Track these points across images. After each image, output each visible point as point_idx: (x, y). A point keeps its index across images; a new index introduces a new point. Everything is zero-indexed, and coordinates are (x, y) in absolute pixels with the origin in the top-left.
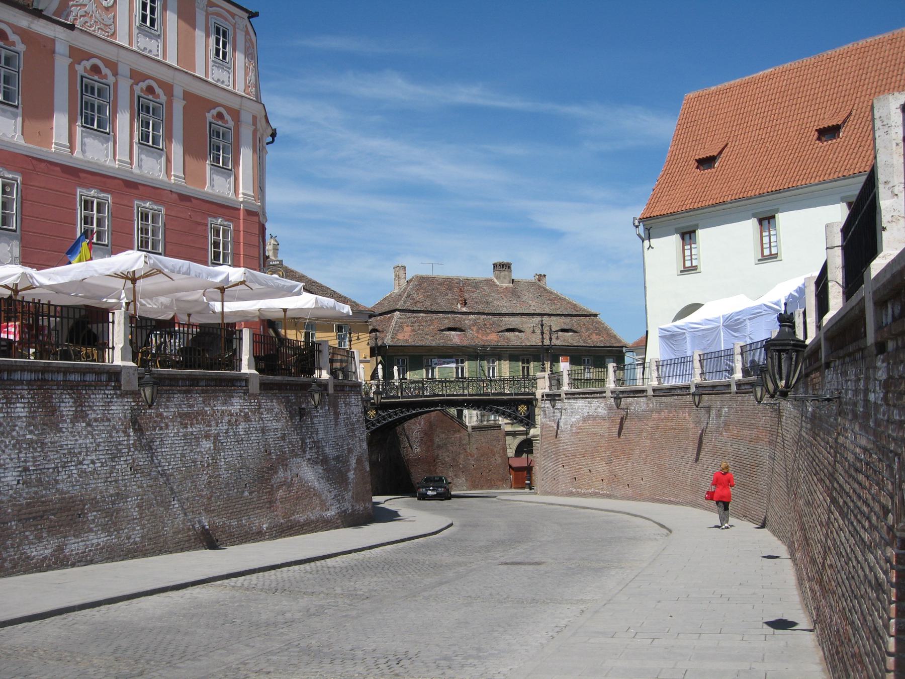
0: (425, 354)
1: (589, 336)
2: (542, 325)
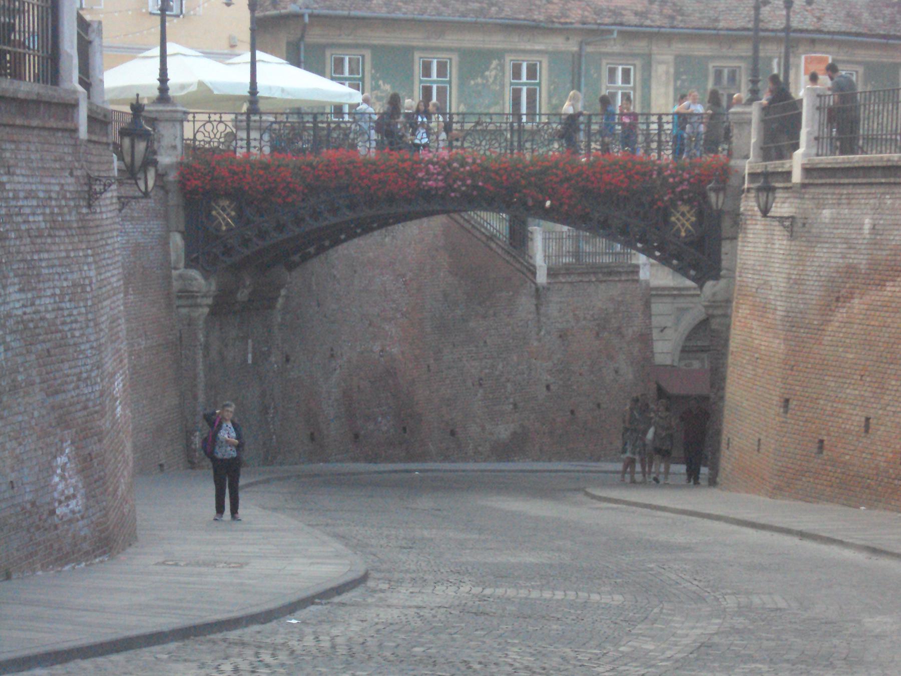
0: (421, 44)
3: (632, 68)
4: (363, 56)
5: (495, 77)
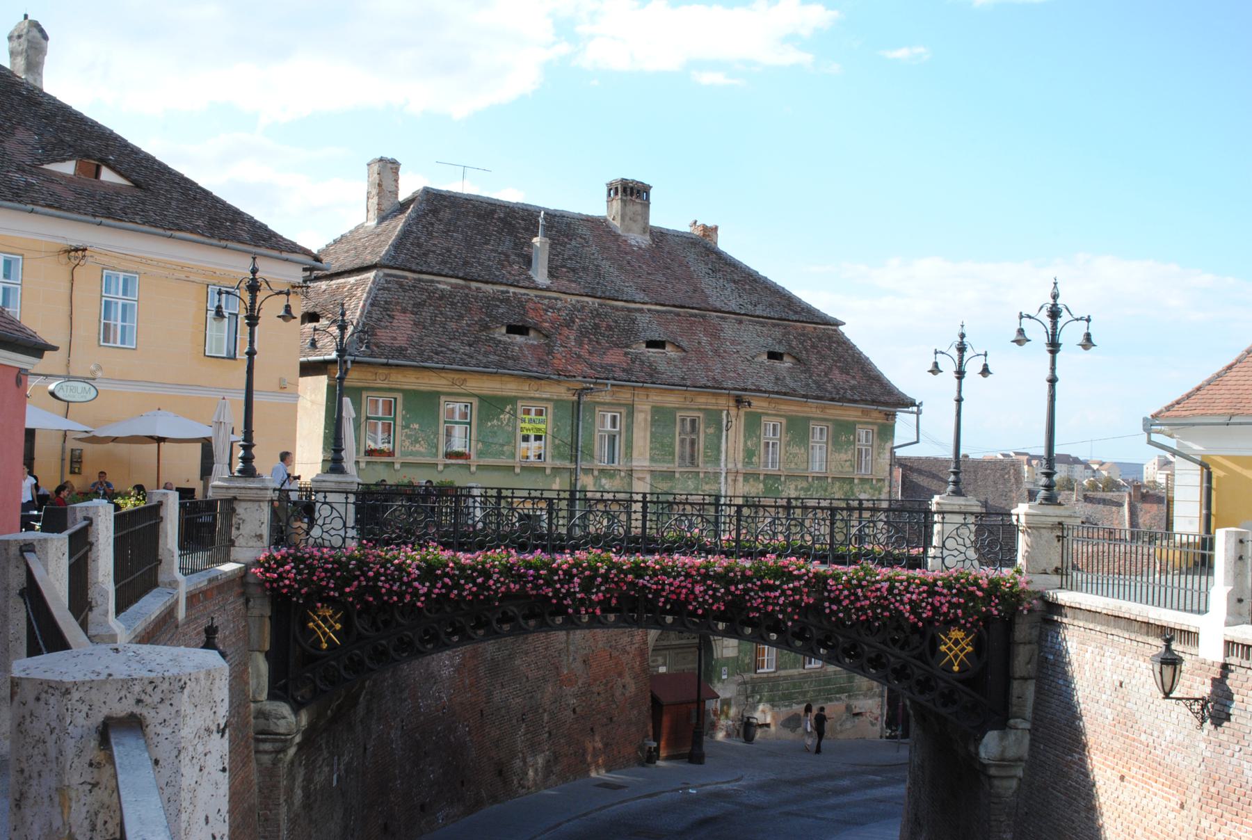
1: (826, 375)
2: (1054, 314)
3: (618, 415)
4: (395, 399)
5: (509, 419)
